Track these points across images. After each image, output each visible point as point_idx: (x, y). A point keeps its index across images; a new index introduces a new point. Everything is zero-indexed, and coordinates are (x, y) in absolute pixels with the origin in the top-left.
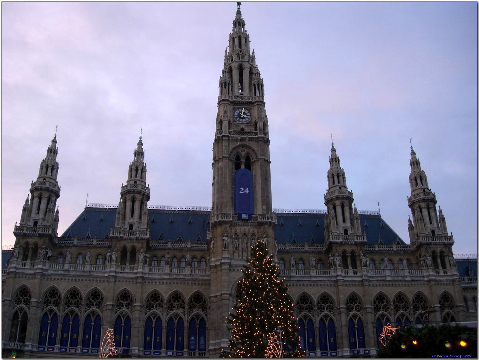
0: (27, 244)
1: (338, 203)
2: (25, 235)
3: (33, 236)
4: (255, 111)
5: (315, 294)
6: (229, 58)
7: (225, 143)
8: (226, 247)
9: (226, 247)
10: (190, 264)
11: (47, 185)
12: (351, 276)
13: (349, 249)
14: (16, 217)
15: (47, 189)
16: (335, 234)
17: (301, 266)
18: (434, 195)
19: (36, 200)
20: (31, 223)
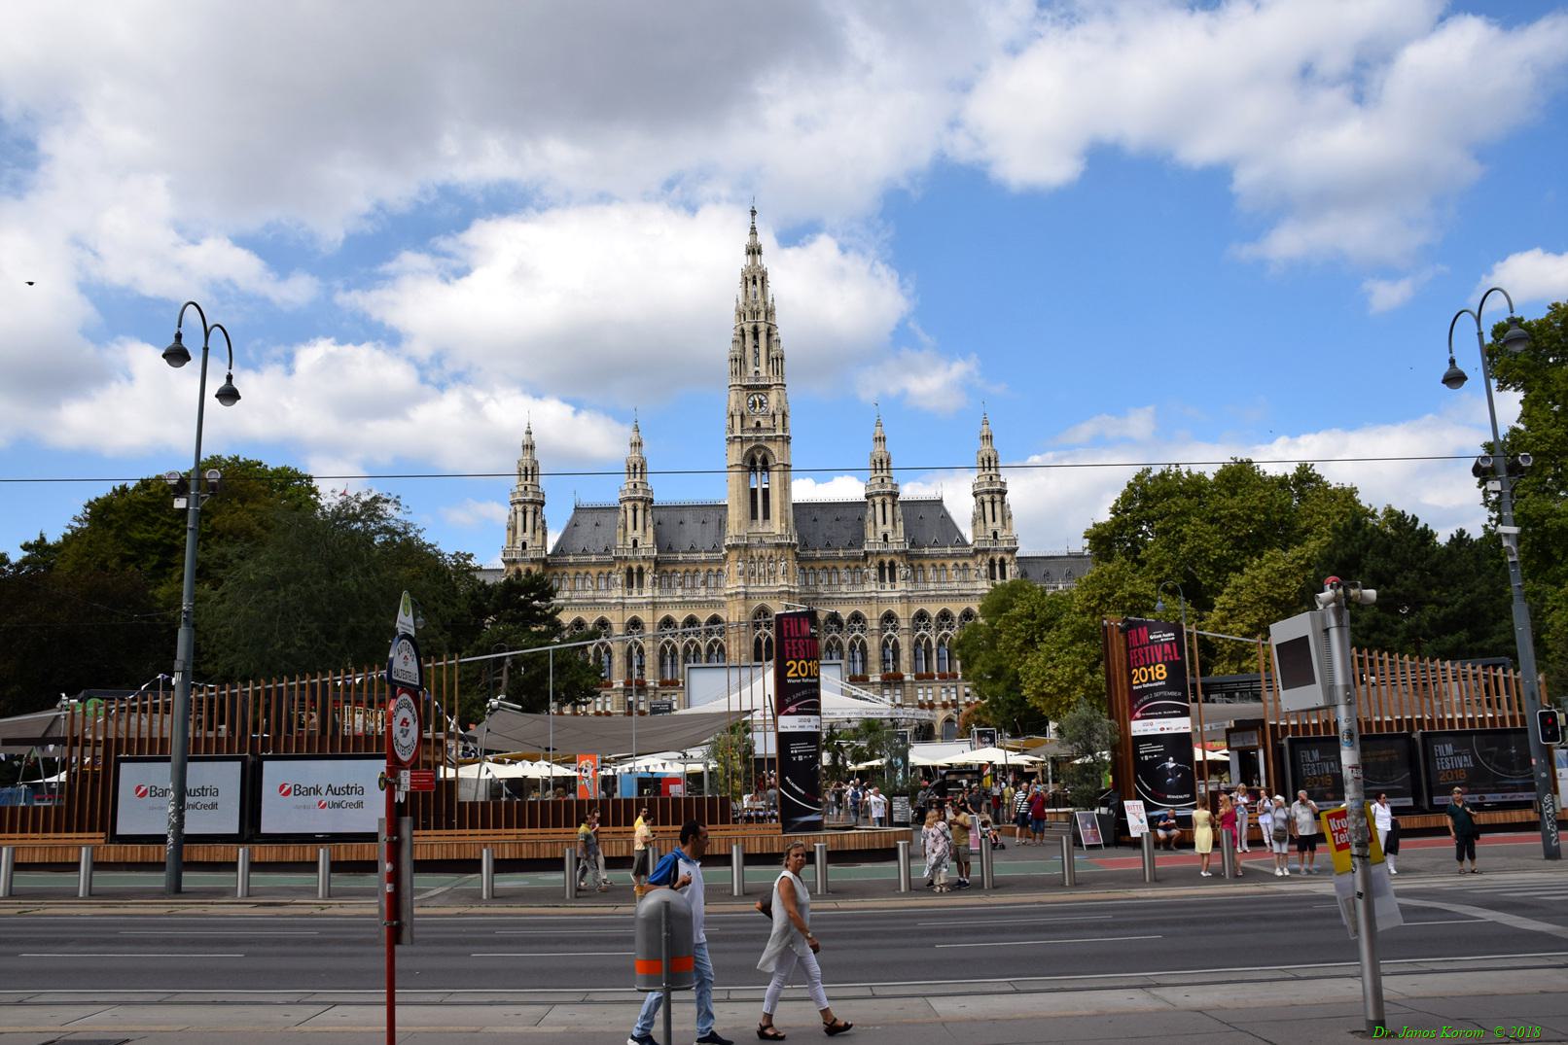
0: (519, 571)
1: (878, 500)
2: (515, 561)
3: (524, 561)
4: (773, 396)
5: (845, 612)
6: (741, 315)
7: (737, 446)
8: (741, 573)
9: (741, 573)
10: (705, 583)
11: (530, 497)
12: (888, 590)
13: (887, 560)
14: (503, 539)
15: (532, 502)
16: (872, 542)
17: (835, 580)
18: (1003, 484)
19: (520, 516)
20: (519, 544)
